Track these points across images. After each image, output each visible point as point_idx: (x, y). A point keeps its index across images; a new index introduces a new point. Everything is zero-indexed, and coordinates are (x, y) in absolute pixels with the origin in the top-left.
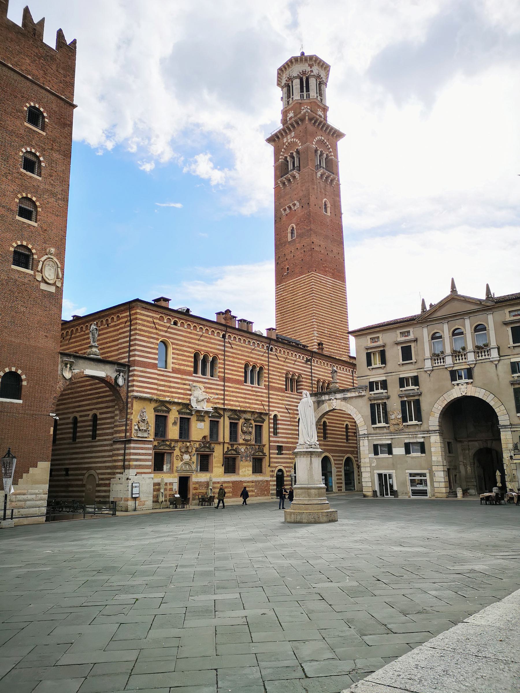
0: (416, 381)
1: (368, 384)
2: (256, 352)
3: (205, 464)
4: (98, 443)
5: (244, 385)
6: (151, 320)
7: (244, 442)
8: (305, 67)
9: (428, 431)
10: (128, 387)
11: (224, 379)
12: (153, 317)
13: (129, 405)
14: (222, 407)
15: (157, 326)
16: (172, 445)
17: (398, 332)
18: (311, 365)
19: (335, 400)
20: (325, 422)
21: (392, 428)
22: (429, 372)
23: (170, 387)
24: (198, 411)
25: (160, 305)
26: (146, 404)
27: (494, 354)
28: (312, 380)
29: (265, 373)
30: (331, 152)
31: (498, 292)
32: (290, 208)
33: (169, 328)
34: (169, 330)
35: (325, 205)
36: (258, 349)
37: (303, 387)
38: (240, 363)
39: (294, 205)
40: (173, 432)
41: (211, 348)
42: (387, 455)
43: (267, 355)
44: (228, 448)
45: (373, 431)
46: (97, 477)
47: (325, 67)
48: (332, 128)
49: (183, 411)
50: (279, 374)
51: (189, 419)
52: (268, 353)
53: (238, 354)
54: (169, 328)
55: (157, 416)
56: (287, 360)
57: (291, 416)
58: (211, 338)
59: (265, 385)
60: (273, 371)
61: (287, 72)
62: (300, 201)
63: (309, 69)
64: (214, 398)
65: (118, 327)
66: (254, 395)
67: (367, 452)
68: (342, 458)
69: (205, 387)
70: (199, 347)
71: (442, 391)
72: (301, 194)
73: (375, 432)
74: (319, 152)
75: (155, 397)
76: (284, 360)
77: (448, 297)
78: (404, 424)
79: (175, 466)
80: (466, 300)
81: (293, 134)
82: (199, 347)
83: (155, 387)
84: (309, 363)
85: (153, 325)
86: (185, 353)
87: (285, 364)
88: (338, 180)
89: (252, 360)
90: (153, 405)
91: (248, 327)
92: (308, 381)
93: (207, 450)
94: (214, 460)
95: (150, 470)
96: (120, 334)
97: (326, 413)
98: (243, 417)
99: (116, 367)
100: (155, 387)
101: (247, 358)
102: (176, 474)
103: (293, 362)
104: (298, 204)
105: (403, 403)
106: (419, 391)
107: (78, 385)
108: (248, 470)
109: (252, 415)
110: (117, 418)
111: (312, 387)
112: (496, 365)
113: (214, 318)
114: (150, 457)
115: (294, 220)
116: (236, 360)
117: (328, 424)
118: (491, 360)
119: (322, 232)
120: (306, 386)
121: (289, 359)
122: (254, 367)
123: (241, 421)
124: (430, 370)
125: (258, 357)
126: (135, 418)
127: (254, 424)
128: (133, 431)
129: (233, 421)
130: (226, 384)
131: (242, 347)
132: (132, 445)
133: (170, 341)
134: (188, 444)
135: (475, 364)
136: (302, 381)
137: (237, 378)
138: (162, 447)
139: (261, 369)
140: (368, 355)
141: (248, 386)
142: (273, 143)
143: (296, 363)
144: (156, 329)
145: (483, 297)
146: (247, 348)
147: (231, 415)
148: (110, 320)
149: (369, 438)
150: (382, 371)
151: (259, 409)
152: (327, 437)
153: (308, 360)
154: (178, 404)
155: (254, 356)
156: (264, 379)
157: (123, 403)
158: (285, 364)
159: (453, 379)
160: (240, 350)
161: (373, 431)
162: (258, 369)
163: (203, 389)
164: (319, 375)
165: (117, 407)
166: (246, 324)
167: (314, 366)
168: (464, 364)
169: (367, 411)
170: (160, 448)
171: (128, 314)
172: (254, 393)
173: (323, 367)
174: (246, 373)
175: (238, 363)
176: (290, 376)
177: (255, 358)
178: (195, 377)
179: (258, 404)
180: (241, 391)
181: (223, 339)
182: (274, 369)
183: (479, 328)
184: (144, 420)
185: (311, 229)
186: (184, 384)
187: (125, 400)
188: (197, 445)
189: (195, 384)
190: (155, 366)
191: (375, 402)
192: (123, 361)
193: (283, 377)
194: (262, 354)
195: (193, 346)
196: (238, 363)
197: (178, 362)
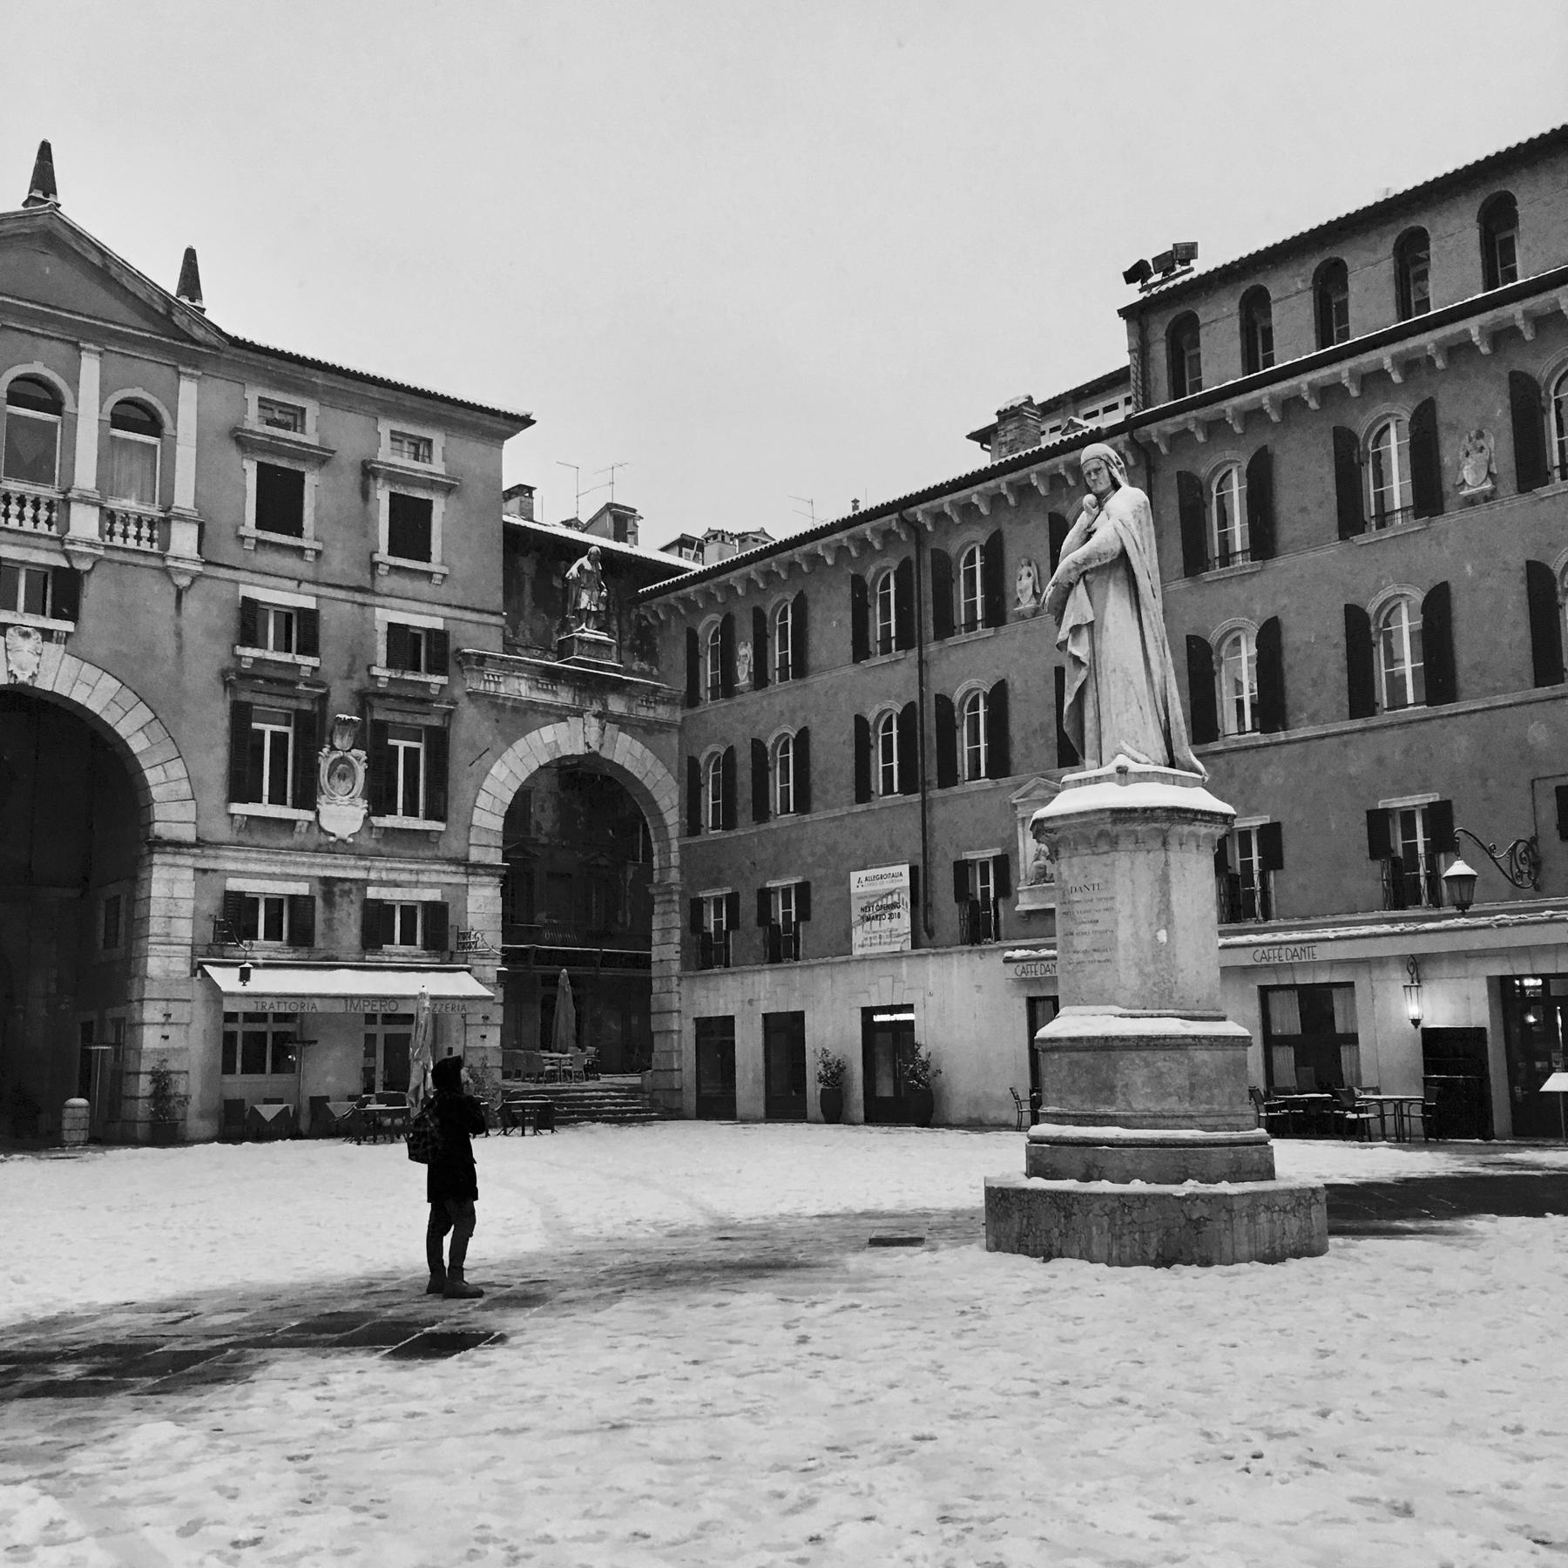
27: (183, 540)
80: (106, 270)
112: (180, 594)
118: (170, 562)
135: (98, 560)
168: (43, 542)
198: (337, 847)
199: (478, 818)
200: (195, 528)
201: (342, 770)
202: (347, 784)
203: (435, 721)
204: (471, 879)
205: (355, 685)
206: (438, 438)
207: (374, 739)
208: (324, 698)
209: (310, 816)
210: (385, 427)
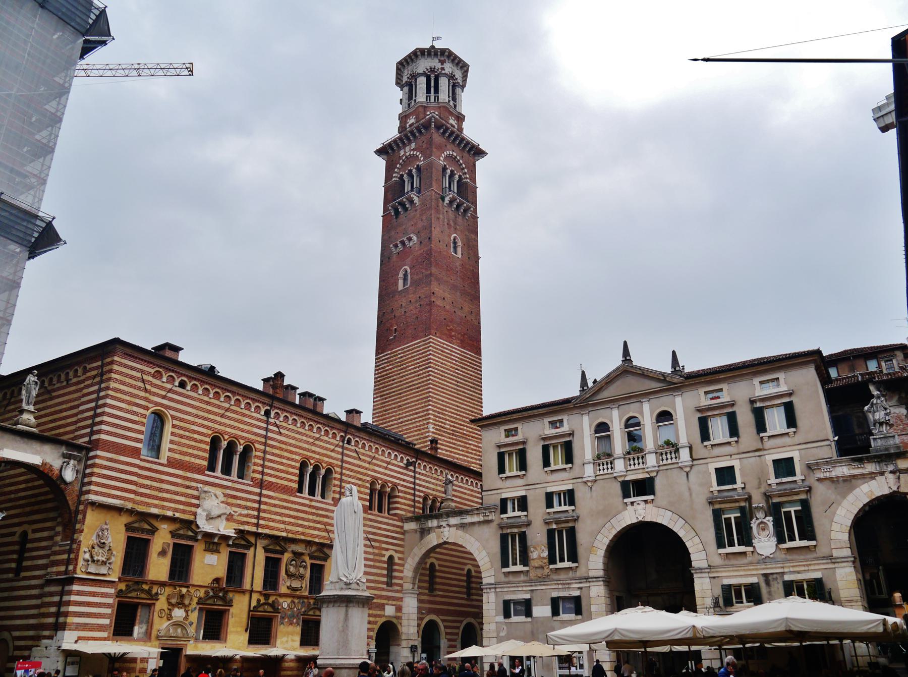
0: (570, 497)
1: (498, 503)
2: (322, 444)
3: (214, 628)
4: (22, 583)
5: (297, 496)
6: (139, 375)
7: (288, 592)
8: (435, 63)
9: (587, 579)
10: (83, 484)
11: (261, 484)
12: (142, 371)
13: (80, 517)
14: (254, 529)
15: (148, 387)
16: (154, 591)
17: (546, 420)
18: (414, 472)
19: (447, 529)
20: (432, 565)
21: (532, 574)
22: (590, 484)
23: (161, 490)
24: (208, 536)
25: (164, 356)
26: (109, 517)
27: (684, 454)
28: (414, 495)
29: (335, 479)
30: (465, 173)
31: (690, 365)
32: (403, 243)
33: (170, 391)
34: (170, 395)
35: (455, 243)
36: (326, 438)
37: (398, 506)
38: (292, 460)
39: (410, 239)
40: (158, 568)
41: (242, 430)
42: (522, 618)
43: (340, 450)
44: (259, 601)
45: (503, 579)
46: (11, 645)
47: (464, 67)
48: (468, 143)
49: (181, 532)
50: (360, 483)
51: (192, 546)
52: (343, 447)
53: (290, 445)
54: (170, 391)
55: (129, 538)
56: (374, 461)
57: (376, 551)
58: (244, 415)
59: (333, 499)
60: (349, 476)
61: (410, 68)
62: (418, 234)
63: (439, 66)
64: (240, 515)
65: (82, 385)
66: (313, 514)
67: (493, 613)
68: (458, 625)
69: (225, 495)
70: (221, 428)
71: (609, 514)
72: (420, 224)
73: (507, 580)
74: (449, 171)
75: (129, 506)
76: (369, 460)
77: (618, 368)
78: (551, 566)
79: (156, 627)
80: (644, 374)
81: (413, 145)
82: (221, 428)
83: (133, 487)
84: (412, 468)
85: (141, 385)
86: (195, 436)
87: (371, 467)
88: (475, 211)
89: (313, 455)
90: (125, 519)
91: (315, 405)
92: (408, 496)
93: (220, 603)
94: (231, 621)
95: (105, 635)
96: (84, 396)
97: (433, 550)
98: (290, 550)
99: (64, 450)
100: (133, 487)
101: (305, 453)
102: (157, 643)
103: (385, 465)
104: (415, 238)
105: (551, 533)
106: (574, 514)
107: (8, 481)
108: (293, 641)
109: (306, 546)
110: (58, 538)
111: (414, 507)
113: (260, 386)
114: (109, 611)
115: (408, 261)
116: (286, 454)
117: (437, 568)
118: (680, 464)
119: (449, 279)
120: (404, 504)
121: (377, 459)
122: (316, 468)
123: (287, 556)
124: (592, 481)
125: (325, 452)
126: (87, 539)
127: (309, 561)
128: (81, 562)
129: (272, 555)
130: (264, 492)
131: (299, 433)
132: (75, 587)
133: (169, 413)
134: (184, 590)
135: (658, 472)
136: (398, 497)
137: (286, 483)
138: (134, 594)
139: (329, 472)
140: (501, 456)
141: (304, 498)
142: (385, 157)
143: (390, 466)
144: (146, 390)
145: (668, 369)
146: (306, 435)
147: (269, 545)
148: (71, 374)
149: (498, 590)
150: (520, 482)
151: (321, 537)
152: (436, 590)
153: (409, 464)
154: (172, 520)
155: (317, 449)
156: (333, 488)
157: (70, 513)
158: (371, 467)
159: (626, 495)
160: (294, 438)
161: (503, 579)
162: (323, 471)
163: (222, 498)
164: (428, 488)
165: (59, 520)
166: (312, 400)
167: (419, 473)
168: (641, 471)
169: (495, 546)
170: (130, 595)
171: (99, 363)
172: (314, 511)
173: (435, 476)
174: (301, 476)
175: (288, 459)
176: (378, 487)
177: (319, 454)
178: (208, 476)
179: (319, 529)
180: (290, 505)
181: (265, 418)
182: (351, 474)
183: (664, 416)
184: (104, 543)
185: (431, 274)
186: (188, 487)
187: (73, 508)
188: (201, 593)
189: (207, 488)
190: (135, 453)
191: (509, 531)
192: (81, 441)
193: (366, 487)
194: (332, 447)
195: (211, 424)
196: (288, 459)
197: (181, 448)
198: (766, 560)
199: (834, 535)
200: (688, 449)
201: (763, 527)
202: (766, 532)
203: (803, 497)
204: (836, 565)
205: (763, 490)
206: (781, 375)
207: (774, 510)
208: (749, 499)
209: (751, 549)
210: (756, 381)
